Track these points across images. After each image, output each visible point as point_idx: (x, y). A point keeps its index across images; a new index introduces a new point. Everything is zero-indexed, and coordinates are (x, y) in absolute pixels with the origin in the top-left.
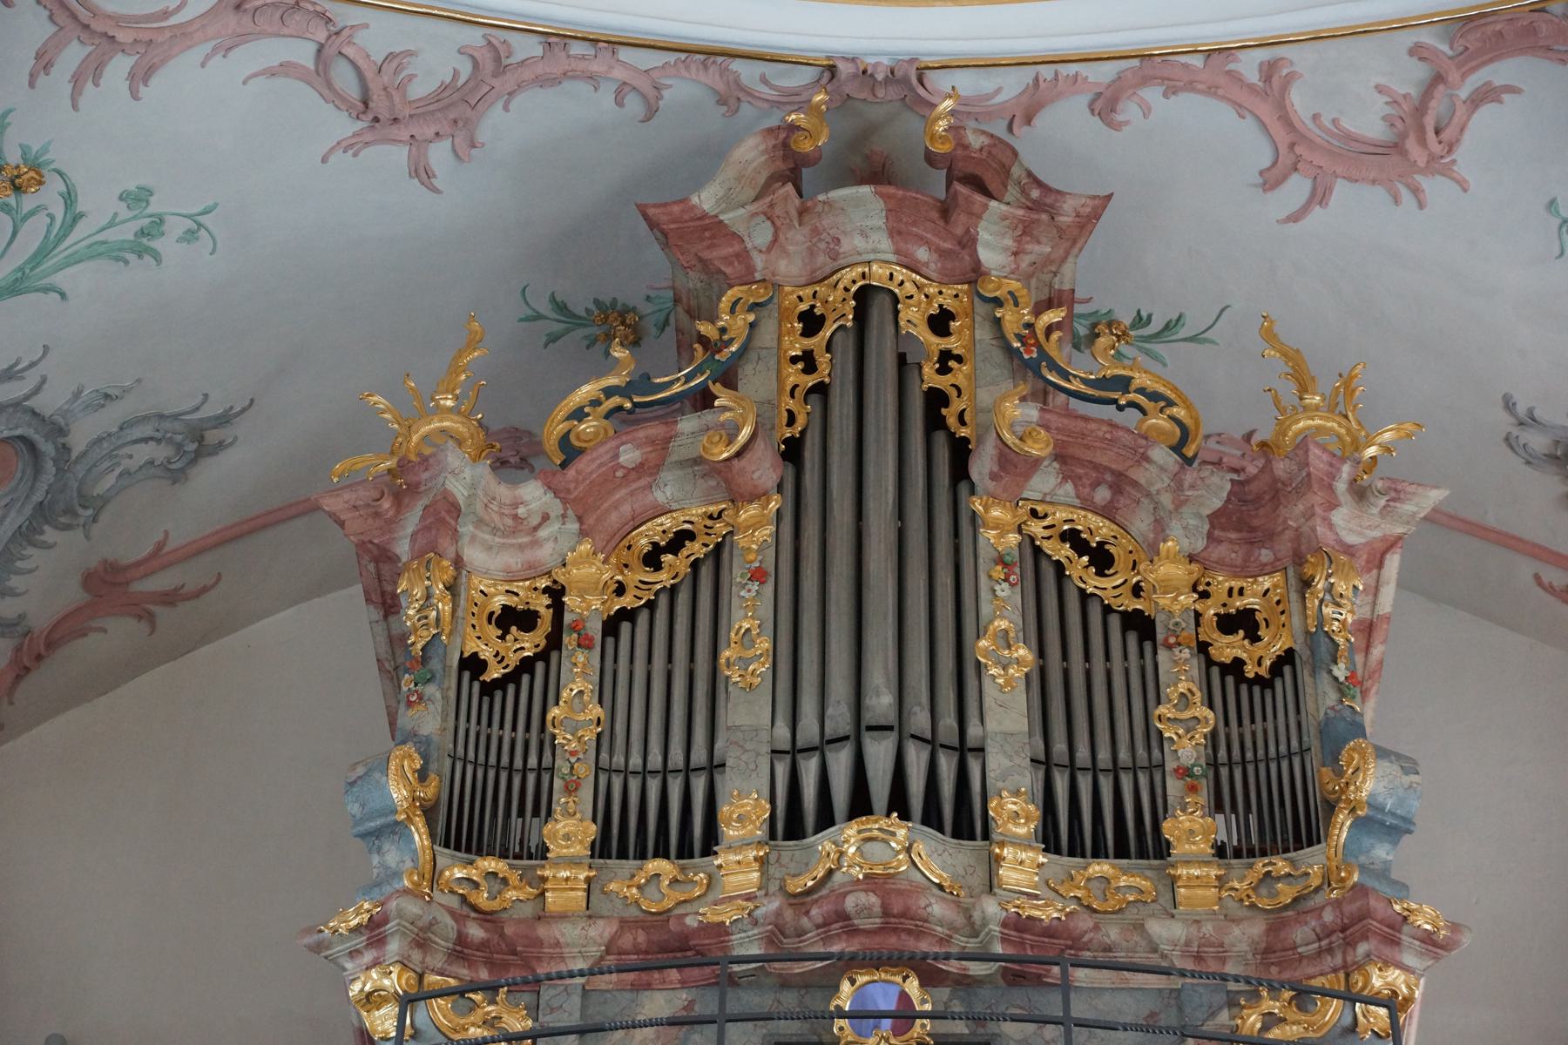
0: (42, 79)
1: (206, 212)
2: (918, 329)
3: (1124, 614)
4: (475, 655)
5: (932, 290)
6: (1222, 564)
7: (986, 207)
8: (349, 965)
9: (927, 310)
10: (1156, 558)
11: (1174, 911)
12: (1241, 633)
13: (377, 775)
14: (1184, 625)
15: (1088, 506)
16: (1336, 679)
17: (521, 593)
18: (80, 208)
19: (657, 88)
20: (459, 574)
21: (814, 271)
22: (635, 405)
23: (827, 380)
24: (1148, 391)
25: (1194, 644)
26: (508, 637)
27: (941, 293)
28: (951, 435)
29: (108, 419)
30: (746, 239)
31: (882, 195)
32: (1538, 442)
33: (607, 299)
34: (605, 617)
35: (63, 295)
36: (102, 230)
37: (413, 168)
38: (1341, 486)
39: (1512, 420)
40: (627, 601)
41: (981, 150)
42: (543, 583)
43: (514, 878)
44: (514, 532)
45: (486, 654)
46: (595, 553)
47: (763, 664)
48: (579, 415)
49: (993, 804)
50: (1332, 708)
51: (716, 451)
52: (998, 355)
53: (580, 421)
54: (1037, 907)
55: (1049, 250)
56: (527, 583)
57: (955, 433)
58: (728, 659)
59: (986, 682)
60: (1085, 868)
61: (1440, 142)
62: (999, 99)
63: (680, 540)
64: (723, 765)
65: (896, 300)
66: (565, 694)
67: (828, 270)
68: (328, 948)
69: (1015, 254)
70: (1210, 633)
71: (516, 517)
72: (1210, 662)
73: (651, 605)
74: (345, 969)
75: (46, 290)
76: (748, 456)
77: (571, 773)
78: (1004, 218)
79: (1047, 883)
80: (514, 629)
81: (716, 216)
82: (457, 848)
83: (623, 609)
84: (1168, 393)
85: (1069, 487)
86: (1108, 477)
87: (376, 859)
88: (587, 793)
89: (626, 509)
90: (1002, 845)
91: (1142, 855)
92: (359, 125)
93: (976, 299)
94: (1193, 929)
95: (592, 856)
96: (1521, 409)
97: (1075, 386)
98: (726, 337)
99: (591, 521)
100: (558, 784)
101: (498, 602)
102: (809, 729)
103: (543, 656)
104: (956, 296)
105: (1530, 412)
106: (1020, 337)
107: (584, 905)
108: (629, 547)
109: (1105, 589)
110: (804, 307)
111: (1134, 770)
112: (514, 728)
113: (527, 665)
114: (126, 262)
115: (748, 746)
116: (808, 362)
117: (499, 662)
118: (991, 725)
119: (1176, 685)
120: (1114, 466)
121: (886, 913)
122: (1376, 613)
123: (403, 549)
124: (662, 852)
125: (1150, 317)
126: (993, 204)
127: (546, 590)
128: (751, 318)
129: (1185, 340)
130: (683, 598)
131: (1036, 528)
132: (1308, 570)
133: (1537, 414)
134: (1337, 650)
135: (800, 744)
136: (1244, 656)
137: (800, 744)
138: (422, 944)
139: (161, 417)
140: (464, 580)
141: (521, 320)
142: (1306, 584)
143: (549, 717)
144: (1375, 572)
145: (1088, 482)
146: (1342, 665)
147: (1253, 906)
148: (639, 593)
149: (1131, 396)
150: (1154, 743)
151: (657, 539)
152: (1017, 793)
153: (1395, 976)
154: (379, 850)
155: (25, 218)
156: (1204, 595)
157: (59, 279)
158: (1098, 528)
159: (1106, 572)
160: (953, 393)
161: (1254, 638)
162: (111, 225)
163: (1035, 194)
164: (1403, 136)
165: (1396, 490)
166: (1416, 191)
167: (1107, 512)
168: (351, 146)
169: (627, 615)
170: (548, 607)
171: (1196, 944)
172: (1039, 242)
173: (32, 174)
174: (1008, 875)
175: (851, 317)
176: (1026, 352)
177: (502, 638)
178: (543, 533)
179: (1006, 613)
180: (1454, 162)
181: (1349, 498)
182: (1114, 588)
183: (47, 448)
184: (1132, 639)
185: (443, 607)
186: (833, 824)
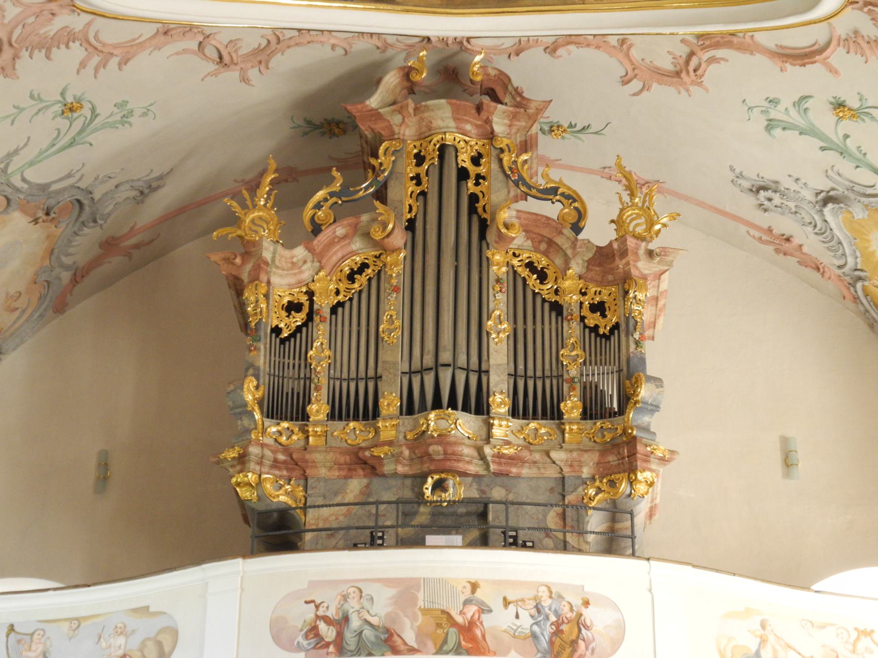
0: (82, 71)
1: (151, 105)
2: (467, 163)
3: (551, 302)
4: (277, 326)
5: (473, 143)
6: (592, 280)
7: (496, 108)
8: (231, 470)
9: (470, 153)
10: (565, 277)
11: (563, 445)
12: (599, 314)
13: (239, 391)
14: (575, 310)
15: (536, 250)
16: (635, 339)
17: (295, 295)
18: (97, 112)
19: (350, 45)
20: (269, 288)
21: (421, 134)
22: (343, 202)
23: (426, 190)
24: (566, 194)
25: (578, 320)
26: (291, 316)
27: (477, 143)
28: (479, 217)
29: (110, 185)
30: (391, 120)
31: (450, 104)
32: (746, 184)
33: (330, 119)
34: (331, 306)
35: (91, 145)
36: (107, 118)
37: (242, 79)
38: (641, 252)
39: (734, 175)
40: (340, 298)
41: (495, 76)
42: (304, 289)
43: (296, 430)
44: (292, 269)
45: (282, 325)
46: (327, 276)
47: (398, 332)
48: (318, 206)
49: (491, 399)
50: (632, 352)
51: (377, 235)
52: (501, 176)
53: (319, 209)
54: (506, 449)
55: (524, 124)
56: (298, 290)
57: (481, 216)
58: (383, 329)
59: (491, 340)
60: (528, 425)
61: (696, 75)
62: (504, 47)
63: (364, 266)
64: (381, 377)
65: (457, 151)
66: (315, 344)
67: (427, 134)
68: (222, 463)
69: (510, 126)
70: (586, 312)
71: (293, 263)
72: (585, 326)
73: (351, 299)
74: (229, 472)
75: (83, 143)
76: (392, 236)
77: (318, 382)
78: (504, 112)
79: (512, 431)
80: (293, 312)
81: (377, 110)
82: (272, 418)
83: (339, 302)
84: (575, 196)
85: (529, 242)
86: (546, 239)
87: (239, 422)
88: (324, 391)
89: (340, 255)
90: (493, 418)
91: (552, 419)
92: (217, 67)
93: (492, 147)
94: (569, 455)
95: (328, 420)
96: (738, 171)
97: (534, 192)
98: (382, 168)
99: (324, 261)
100: (313, 386)
101: (285, 301)
102: (416, 365)
103: (305, 325)
104: (484, 145)
105: (741, 174)
106: (511, 169)
107: (325, 444)
108: (341, 271)
109: (543, 290)
110: (415, 151)
111: (551, 377)
112: (294, 359)
113: (299, 329)
114: (117, 128)
115: (391, 371)
116: (417, 179)
117: (287, 328)
118: (492, 361)
119: (570, 339)
120: (548, 236)
121: (445, 453)
122: (661, 290)
123: (245, 277)
124: (356, 418)
125: (576, 125)
126: (499, 106)
127: (306, 293)
128: (393, 158)
129: (592, 133)
130: (364, 296)
131: (515, 262)
132: (626, 286)
133: (744, 174)
134: (637, 325)
135: (413, 370)
136: (599, 324)
137: (413, 370)
138: (260, 463)
139: (133, 181)
140: (271, 291)
141: (291, 128)
142: (626, 293)
143: (309, 355)
144: (657, 281)
145: (537, 241)
146: (638, 333)
147: (595, 441)
148: (345, 294)
149: (558, 197)
150: (560, 365)
151: (353, 267)
152: (501, 393)
153: (648, 475)
154: (241, 419)
155: (75, 120)
156: (584, 294)
157: (89, 139)
158: (542, 262)
159: (544, 282)
160: (481, 195)
161: (604, 316)
162: (111, 115)
163: (518, 99)
164: (681, 71)
165: (665, 252)
166: (688, 90)
167: (545, 254)
168: (215, 74)
169: (340, 304)
170: (307, 300)
171: (570, 461)
172: (520, 121)
173: (78, 105)
174: (498, 432)
175: (437, 159)
176: (513, 176)
177: (288, 316)
178: (304, 267)
179: (500, 306)
180: (702, 82)
181: (645, 256)
182: (547, 289)
183: (86, 202)
184: (554, 315)
185: (263, 306)
186: (426, 410)
